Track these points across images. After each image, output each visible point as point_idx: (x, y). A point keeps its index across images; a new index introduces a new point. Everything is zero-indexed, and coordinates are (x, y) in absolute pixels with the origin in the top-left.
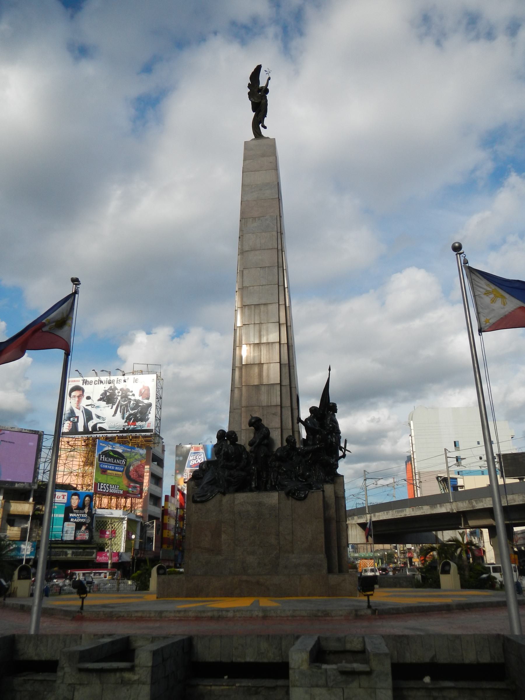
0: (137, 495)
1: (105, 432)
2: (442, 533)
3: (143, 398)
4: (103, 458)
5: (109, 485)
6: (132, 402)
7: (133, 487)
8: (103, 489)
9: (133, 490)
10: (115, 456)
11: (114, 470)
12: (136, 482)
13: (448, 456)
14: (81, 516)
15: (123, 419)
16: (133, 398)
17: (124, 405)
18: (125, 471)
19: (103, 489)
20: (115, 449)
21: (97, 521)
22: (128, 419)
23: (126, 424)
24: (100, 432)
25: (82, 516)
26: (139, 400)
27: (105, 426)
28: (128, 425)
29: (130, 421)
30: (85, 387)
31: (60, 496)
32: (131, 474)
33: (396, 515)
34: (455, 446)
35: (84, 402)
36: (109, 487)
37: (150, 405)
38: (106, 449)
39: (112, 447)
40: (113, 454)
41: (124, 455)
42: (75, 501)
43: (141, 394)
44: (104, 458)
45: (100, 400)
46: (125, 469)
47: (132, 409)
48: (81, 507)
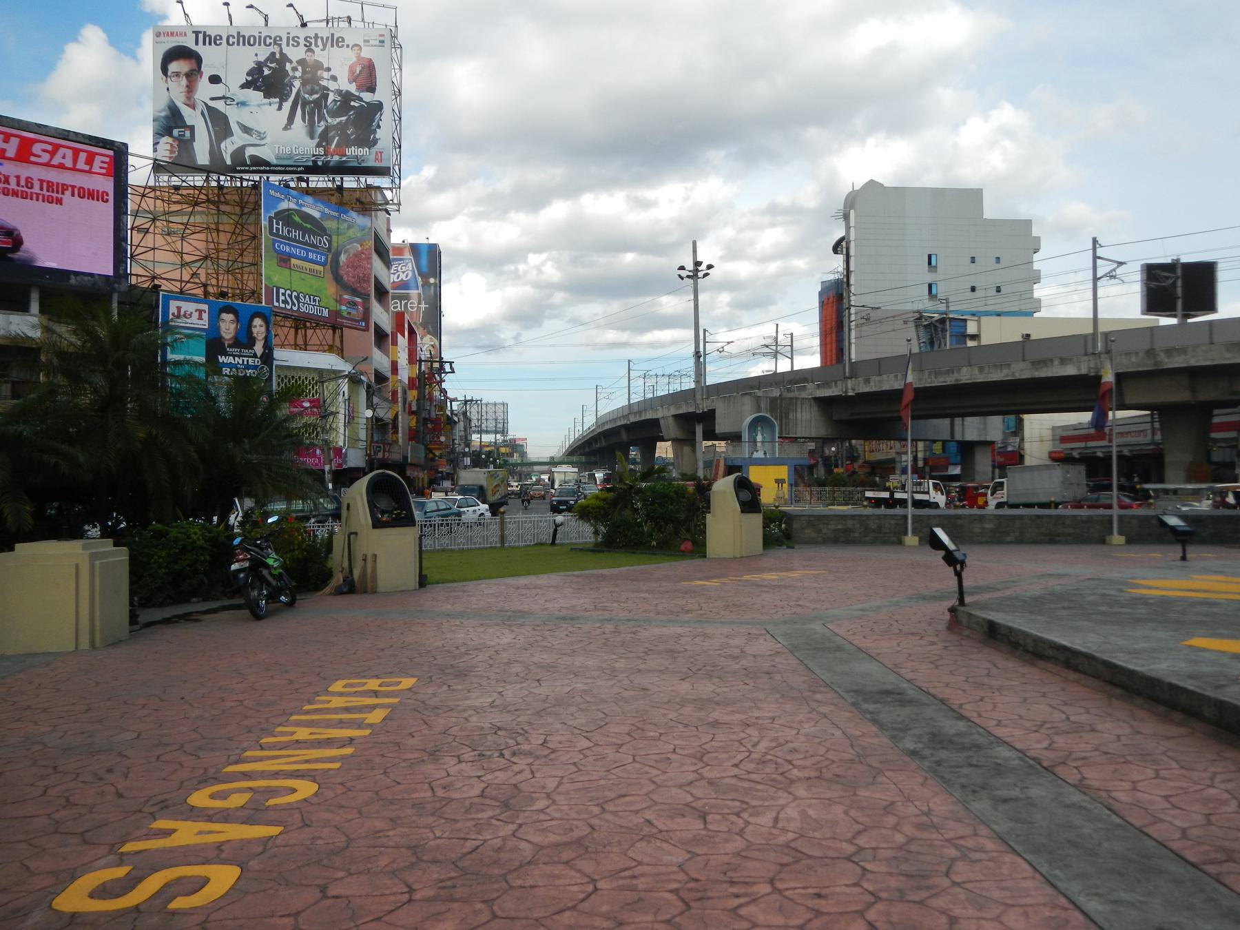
0: (358, 321)
1: (268, 168)
2: (963, 421)
3: (359, 88)
4: (279, 226)
5: (299, 295)
6: (331, 97)
7: (349, 303)
8: (285, 302)
9: (349, 310)
10: (305, 225)
11: (306, 259)
12: (355, 292)
13: (1098, 254)
14: (245, 363)
15: (312, 137)
16: (332, 86)
17: (311, 102)
18: (329, 264)
19: (285, 302)
20: (304, 209)
21: (279, 376)
22: (325, 138)
23: (322, 152)
24: (254, 168)
25: (250, 363)
26: (348, 93)
27: (266, 153)
28: (326, 154)
29: (329, 142)
30: (201, 49)
31: (192, 313)
32: (342, 272)
33: (929, 380)
34: (930, 263)
35: (205, 90)
36: (298, 298)
37: (379, 107)
38: (284, 205)
39: (297, 203)
40: (300, 222)
41: (326, 226)
42: (228, 327)
43: (353, 79)
44: (280, 227)
45: (245, 86)
46: (329, 260)
47: (334, 114)
48: (245, 340)
